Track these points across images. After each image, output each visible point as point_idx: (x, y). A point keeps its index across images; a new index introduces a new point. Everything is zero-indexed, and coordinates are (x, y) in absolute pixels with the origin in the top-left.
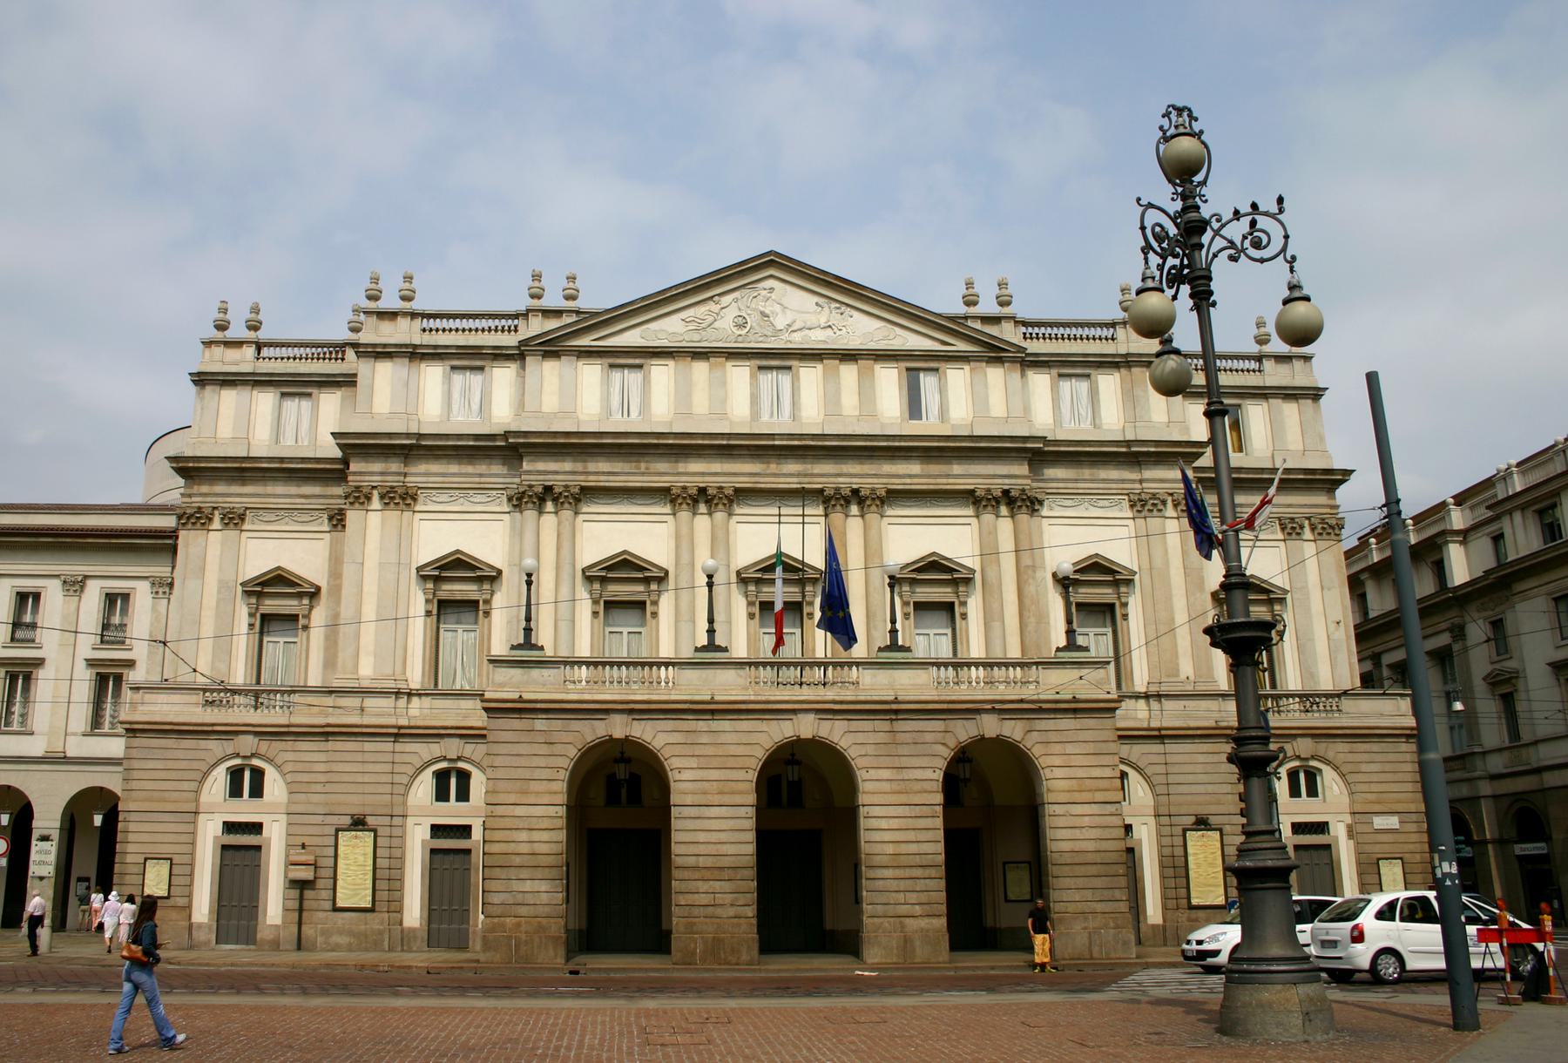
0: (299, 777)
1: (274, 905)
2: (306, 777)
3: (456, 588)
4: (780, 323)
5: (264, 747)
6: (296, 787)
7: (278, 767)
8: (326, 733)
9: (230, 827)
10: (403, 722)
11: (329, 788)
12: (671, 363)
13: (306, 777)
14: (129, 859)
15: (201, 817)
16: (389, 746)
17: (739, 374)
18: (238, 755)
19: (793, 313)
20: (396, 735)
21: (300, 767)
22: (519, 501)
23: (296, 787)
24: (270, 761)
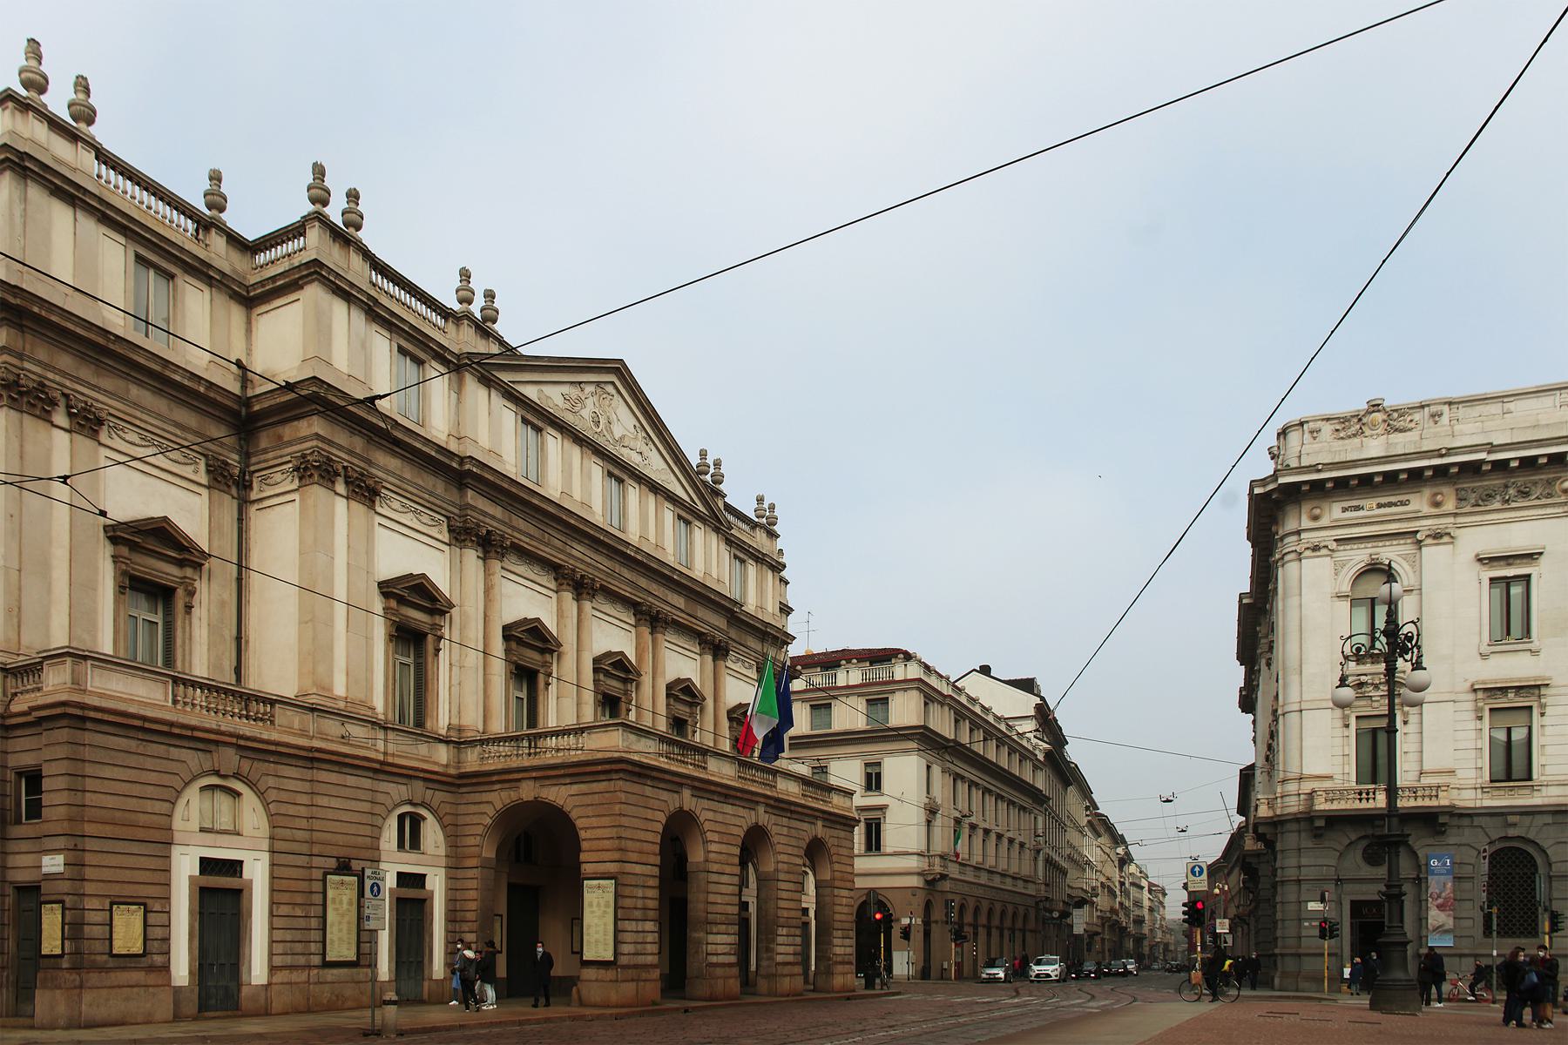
0: (284, 809)
1: (257, 969)
2: (292, 810)
3: (414, 613)
4: (618, 432)
5: (246, 766)
6: (281, 821)
7: (261, 795)
8: (312, 759)
9: (207, 865)
10: (381, 757)
11: (317, 825)
12: (559, 436)
13: (292, 810)
14: (90, 903)
15: (176, 851)
16: (367, 783)
17: (597, 470)
18: (217, 773)
19: (621, 426)
20: (375, 771)
21: (284, 796)
22: (463, 533)
23: (281, 821)
24: (252, 785)
